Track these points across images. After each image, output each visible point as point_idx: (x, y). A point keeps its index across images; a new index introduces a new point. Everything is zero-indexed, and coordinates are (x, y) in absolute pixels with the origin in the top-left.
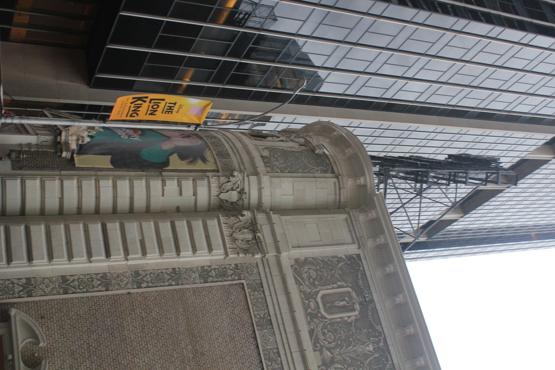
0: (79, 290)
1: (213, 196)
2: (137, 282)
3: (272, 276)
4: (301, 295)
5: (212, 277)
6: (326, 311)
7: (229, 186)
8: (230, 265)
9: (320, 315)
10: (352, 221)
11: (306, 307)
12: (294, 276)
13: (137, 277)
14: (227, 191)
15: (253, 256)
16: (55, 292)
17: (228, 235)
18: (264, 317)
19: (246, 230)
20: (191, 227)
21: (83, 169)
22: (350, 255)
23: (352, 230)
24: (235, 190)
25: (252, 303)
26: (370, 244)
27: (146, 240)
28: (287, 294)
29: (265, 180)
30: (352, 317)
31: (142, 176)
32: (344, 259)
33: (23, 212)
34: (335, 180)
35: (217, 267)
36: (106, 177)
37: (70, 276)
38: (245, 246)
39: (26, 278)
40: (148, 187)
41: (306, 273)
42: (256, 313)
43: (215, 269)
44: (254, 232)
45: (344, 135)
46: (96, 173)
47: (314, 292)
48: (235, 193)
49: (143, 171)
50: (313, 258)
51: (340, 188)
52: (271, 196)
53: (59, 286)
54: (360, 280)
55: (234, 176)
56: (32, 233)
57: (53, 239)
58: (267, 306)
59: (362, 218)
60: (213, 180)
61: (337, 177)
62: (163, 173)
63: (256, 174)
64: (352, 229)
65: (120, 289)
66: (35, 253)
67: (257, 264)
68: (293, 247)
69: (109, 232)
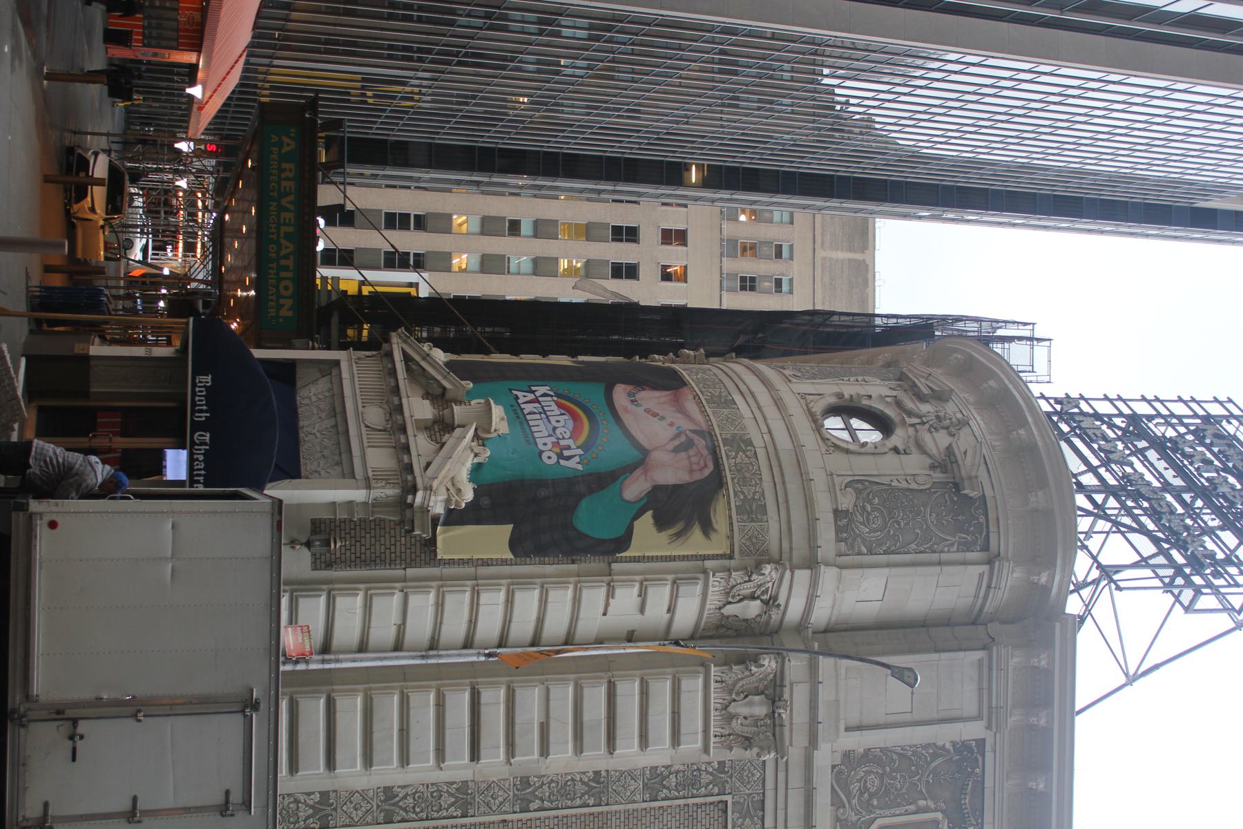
2: (522, 800)
3: (787, 789)
5: (668, 788)
7: (747, 589)
10: (990, 669)
12: (833, 787)
16: (369, 819)
17: (719, 706)
19: (757, 698)
20: (647, 694)
21: (451, 562)
22: (963, 743)
24: (758, 598)
26: (1013, 720)
29: (828, 575)
31: (569, 575)
32: (948, 751)
34: (985, 568)
35: (682, 768)
38: (748, 731)
40: (577, 601)
41: (859, 781)
43: (677, 772)
44: (774, 702)
45: (1040, 443)
46: (475, 573)
49: (573, 562)
51: (989, 587)
53: (378, 806)
56: (338, 715)
57: (375, 727)
61: (990, 562)
62: (614, 566)
63: (812, 563)
64: (985, 685)
66: (340, 756)
68: (847, 729)
69: (484, 710)
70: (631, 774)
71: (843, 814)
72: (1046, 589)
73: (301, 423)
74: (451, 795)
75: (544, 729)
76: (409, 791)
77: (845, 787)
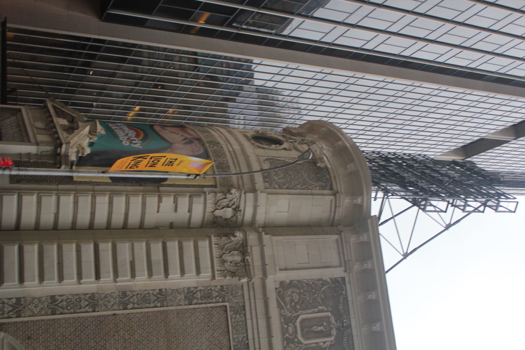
0: (67, 311)
1: (208, 212)
4: (281, 319)
5: (197, 298)
6: (303, 336)
7: (225, 202)
8: (216, 286)
9: (296, 340)
10: (342, 243)
11: (284, 332)
13: (125, 298)
14: (223, 208)
15: (239, 280)
16: (43, 312)
17: (218, 256)
18: (242, 341)
19: (236, 252)
23: (341, 252)
25: (232, 326)
26: (356, 267)
27: (137, 262)
28: (268, 318)
29: (262, 197)
30: (327, 343)
32: (328, 282)
33: (18, 227)
34: (332, 197)
35: (203, 288)
36: (102, 193)
37: (59, 296)
38: (233, 269)
39: (16, 298)
40: (144, 204)
41: (289, 296)
42: (235, 336)
43: (201, 290)
44: (244, 254)
45: (348, 145)
47: (294, 317)
48: (230, 210)
49: (141, 186)
50: (298, 281)
51: (336, 206)
52: (266, 213)
53: (48, 306)
54: (341, 305)
55: (232, 194)
58: (247, 329)
59: (353, 239)
60: (210, 198)
61: (335, 195)
62: (161, 188)
63: (254, 190)
64: (341, 251)
65: (106, 310)
66: (27, 274)
67: (242, 286)
68: (280, 270)
70: (178, 291)
71: (284, 312)
72: (361, 206)
73: (2, 131)
74: (86, 300)
75: (132, 264)
76: (64, 298)
77: (283, 299)
